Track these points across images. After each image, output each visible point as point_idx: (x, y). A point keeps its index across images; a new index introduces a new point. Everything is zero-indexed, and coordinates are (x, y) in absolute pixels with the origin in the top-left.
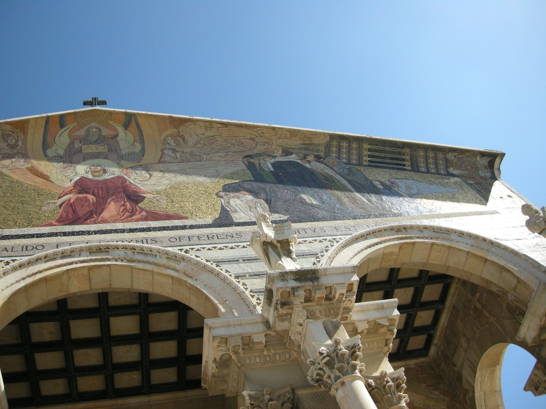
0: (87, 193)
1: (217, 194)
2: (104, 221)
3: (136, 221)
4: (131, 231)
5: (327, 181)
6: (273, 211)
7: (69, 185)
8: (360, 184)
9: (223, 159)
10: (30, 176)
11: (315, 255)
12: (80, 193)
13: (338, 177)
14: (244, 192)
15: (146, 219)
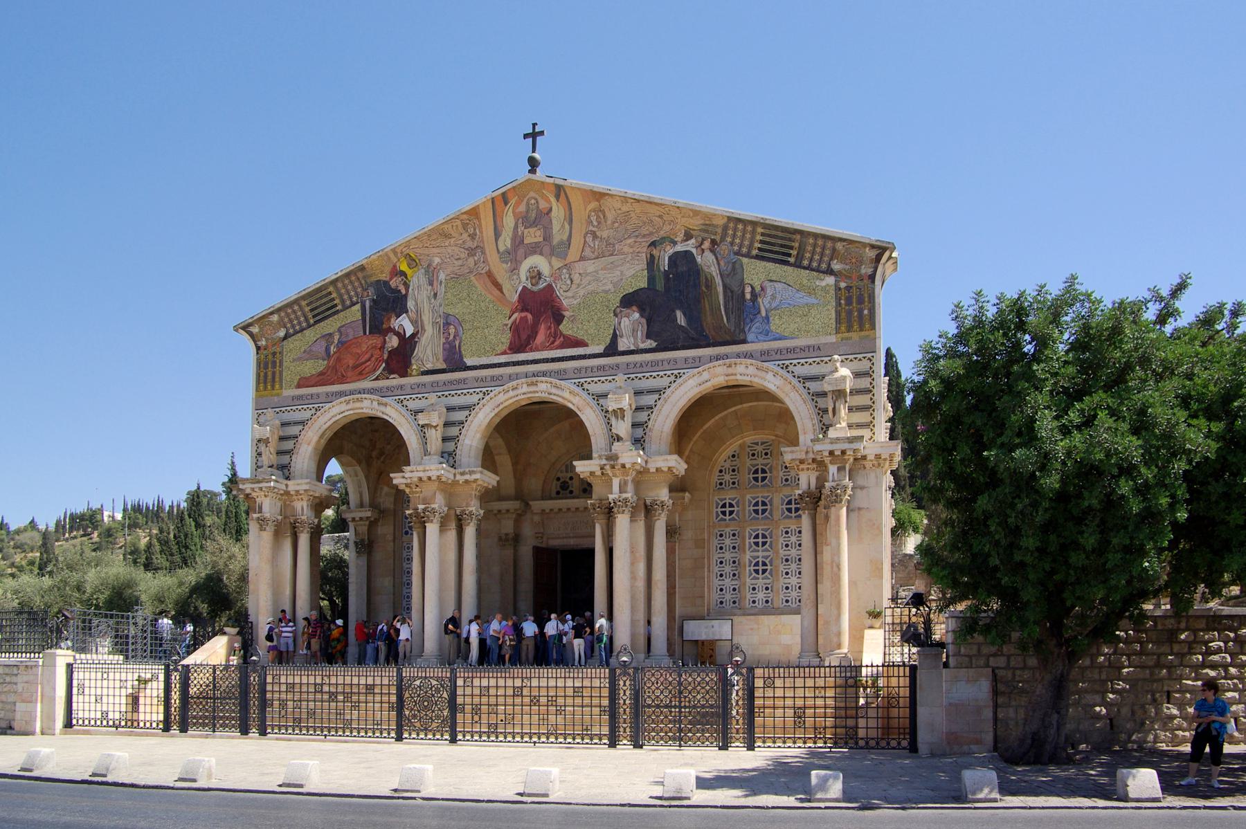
0: (527, 311)
1: (614, 311)
2: (537, 350)
3: (556, 349)
4: (553, 360)
5: (707, 287)
6: (648, 336)
7: (516, 297)
8: (732, 292)
9: (631, 250)
10: (489, 284)
11: (659, 391)
12: (522, 311)
13: (718, 280)
14: (634, 308)
15: (562, 347)
